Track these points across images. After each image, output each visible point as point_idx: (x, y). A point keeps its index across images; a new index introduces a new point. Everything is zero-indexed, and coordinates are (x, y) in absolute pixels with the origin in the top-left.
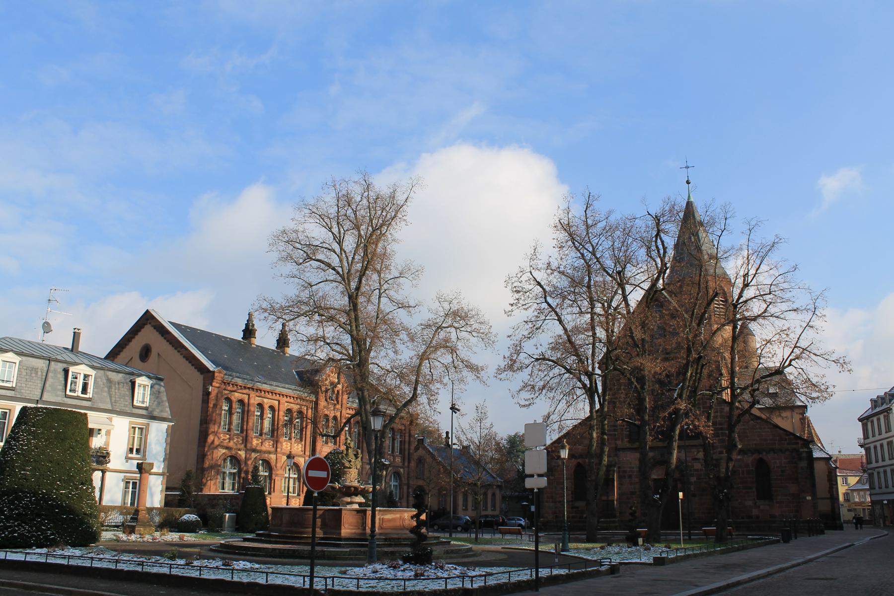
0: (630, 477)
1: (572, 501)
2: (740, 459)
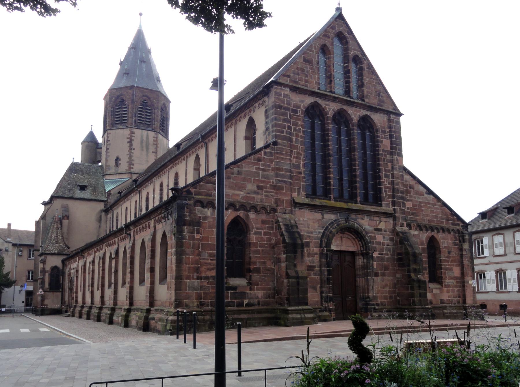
2: (417, 235)
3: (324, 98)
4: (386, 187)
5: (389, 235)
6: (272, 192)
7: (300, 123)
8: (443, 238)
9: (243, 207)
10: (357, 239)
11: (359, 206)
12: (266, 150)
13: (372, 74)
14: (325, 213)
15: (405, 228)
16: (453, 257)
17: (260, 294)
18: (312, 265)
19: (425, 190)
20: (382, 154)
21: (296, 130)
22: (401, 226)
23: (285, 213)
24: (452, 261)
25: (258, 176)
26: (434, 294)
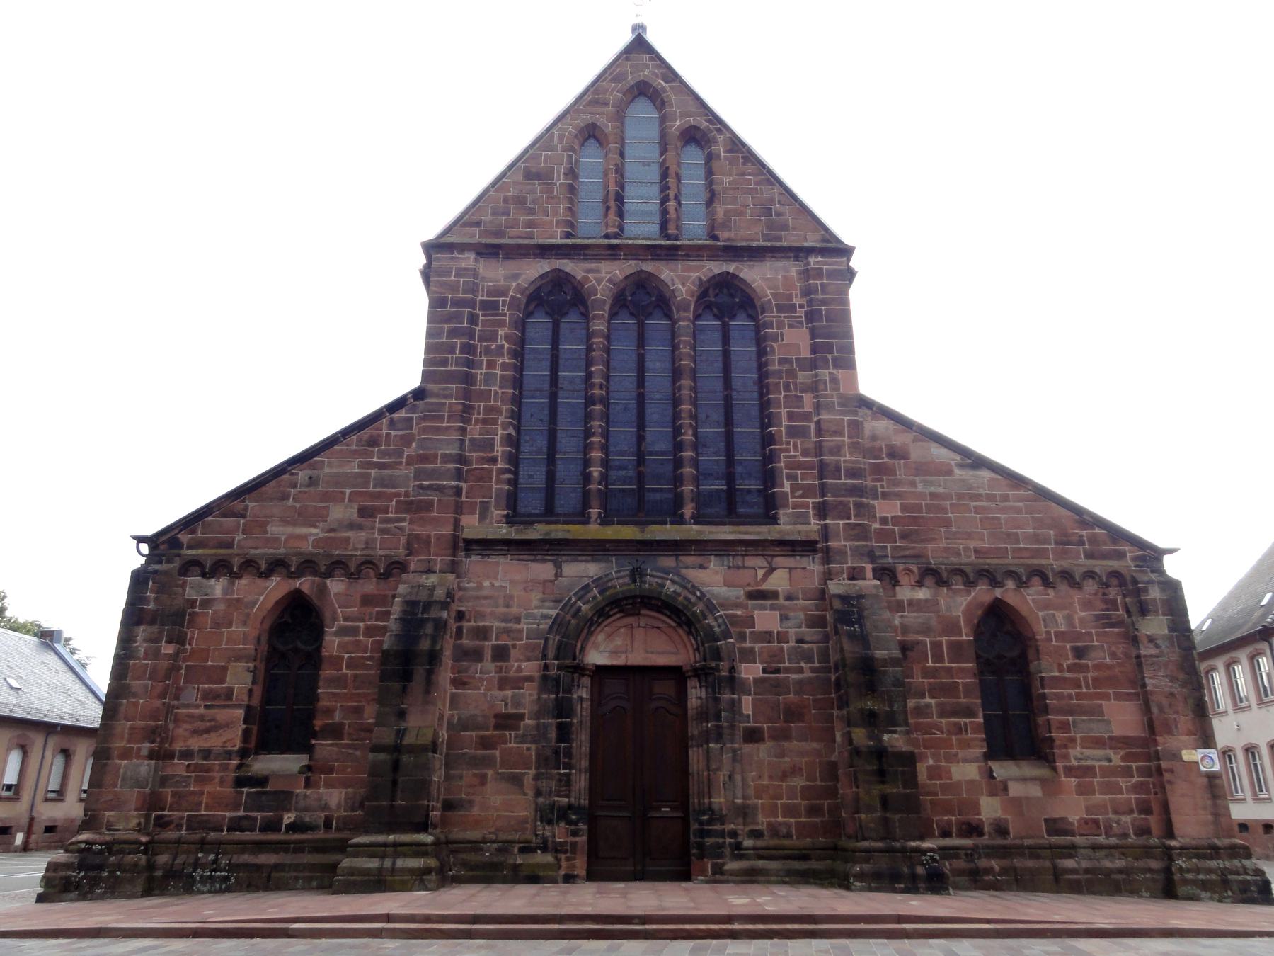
0: (501, 654)
1: (244, 753)
2: (926, 600)
3: (579, 254)
4: (792, 466)
5: (804, 609)
6: (403, 520)
7: (502, 332)
8: (1047, 606)
9: (308, 565)
10: (683, 629)
11: (694, 531)
12: (395, 416)
13: (744, 164)
14: (566, 561)
15: (869, 583)
16: (1098, 667)
17: (335, 798)
18: (514, 711)
19: (958, 457)
20: (780, 371)
21: (488, 351)
22: (852, 578)
23: (429, 571)
24: (1095, 680)
25: (366, 484)
26: (1013, 798)
